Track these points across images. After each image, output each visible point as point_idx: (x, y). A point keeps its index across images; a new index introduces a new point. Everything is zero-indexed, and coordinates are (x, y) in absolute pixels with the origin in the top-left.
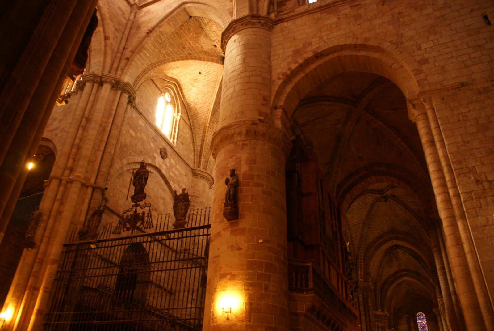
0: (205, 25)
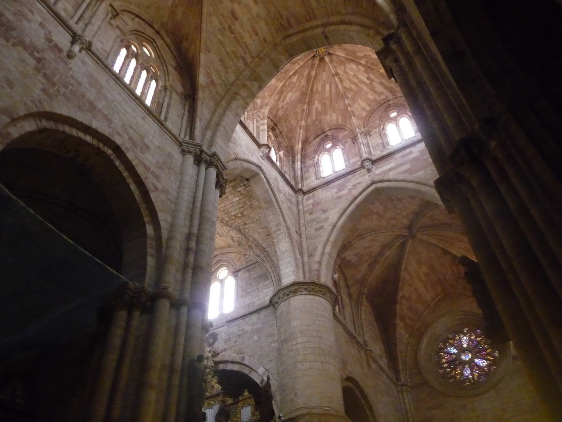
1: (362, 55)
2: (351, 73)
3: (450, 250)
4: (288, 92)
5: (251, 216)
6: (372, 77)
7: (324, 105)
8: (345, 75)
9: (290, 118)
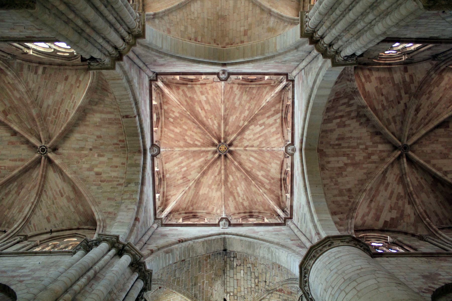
0: (232, 268)
1: (242, 122)
2: (251, 136)
3: (441, 119)
4: (236, 188)
5: (260, 271)
6: (261, 122)
7: (262, 169)
8: (250, 141)
9: (255, 199)
